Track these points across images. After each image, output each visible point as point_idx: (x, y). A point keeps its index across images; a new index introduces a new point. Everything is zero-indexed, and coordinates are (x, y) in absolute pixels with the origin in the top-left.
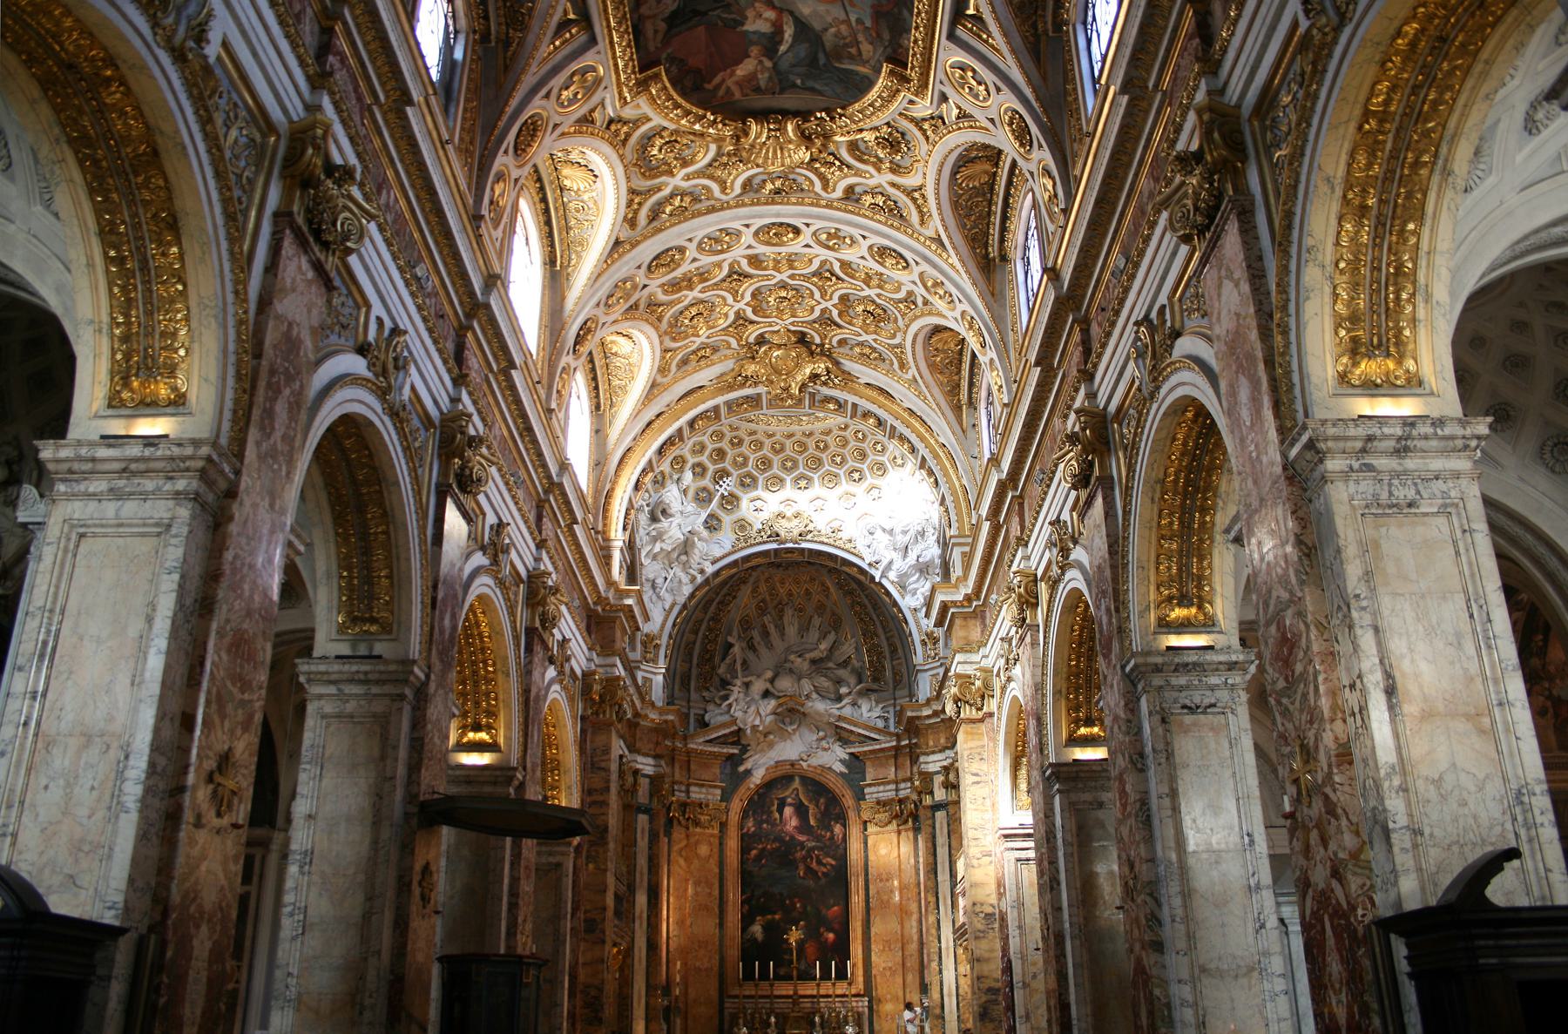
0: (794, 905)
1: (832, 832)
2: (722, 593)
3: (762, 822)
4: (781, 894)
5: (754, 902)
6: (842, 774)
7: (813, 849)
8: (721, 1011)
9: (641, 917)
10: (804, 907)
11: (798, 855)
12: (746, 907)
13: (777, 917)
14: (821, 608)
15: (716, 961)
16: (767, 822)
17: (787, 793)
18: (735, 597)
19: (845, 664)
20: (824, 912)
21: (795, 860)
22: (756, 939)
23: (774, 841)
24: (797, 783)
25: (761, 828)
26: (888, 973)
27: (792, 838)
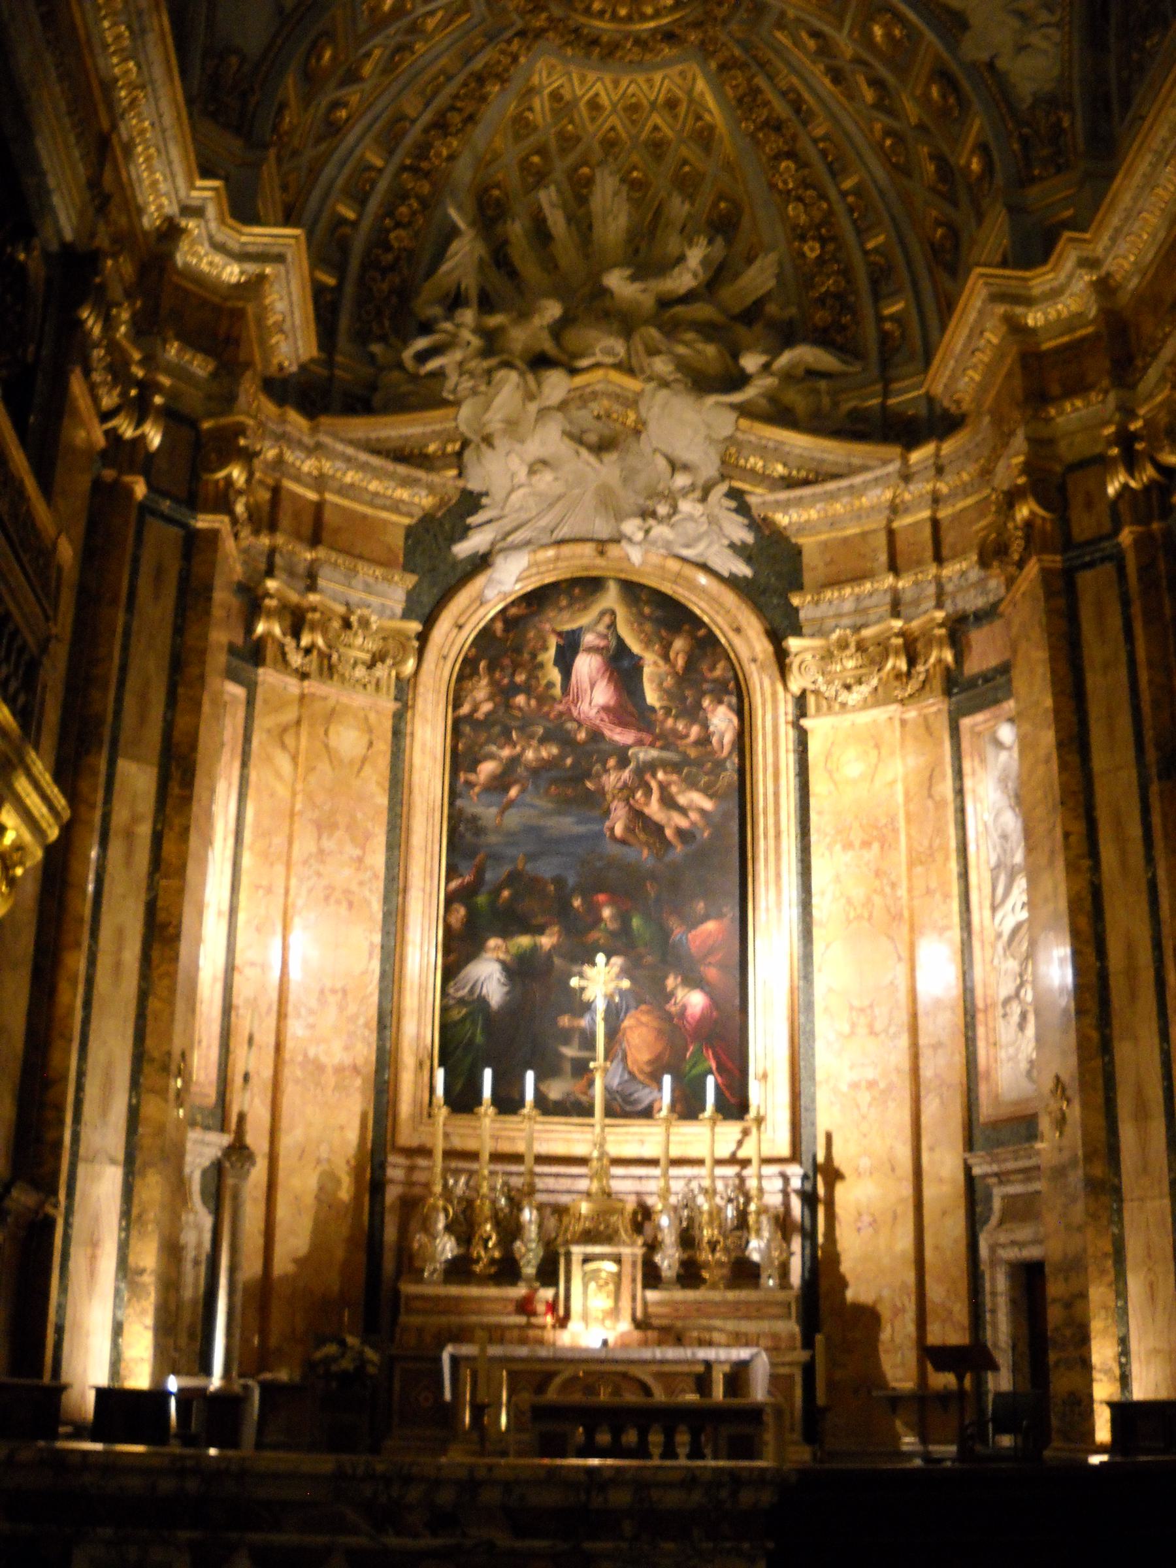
0: (593, 910)
1: (705, 725)
2: (441, 101)
3: (515, 689)
4: (559, 881)
5: (482, 899)
6: (732, 582)
7: (651, 767)
8: (377, 1186)
9: (129, 835)
10: (624, 918)
11: (613, 780)
12: (461, 912)
13: (546, 941)
14: (686, 184)
15: (365, 1052)
16: (527, 689)
17: (584, 620)
18: (471, 119)
19: (751, 315)
20: (678, 932)
21: (602, 792)
22: (483, 1001)
23: (543, 741)
24: (611, 598)
25: (508, 706)
26: (865, 1097)
27: (596, 735)
